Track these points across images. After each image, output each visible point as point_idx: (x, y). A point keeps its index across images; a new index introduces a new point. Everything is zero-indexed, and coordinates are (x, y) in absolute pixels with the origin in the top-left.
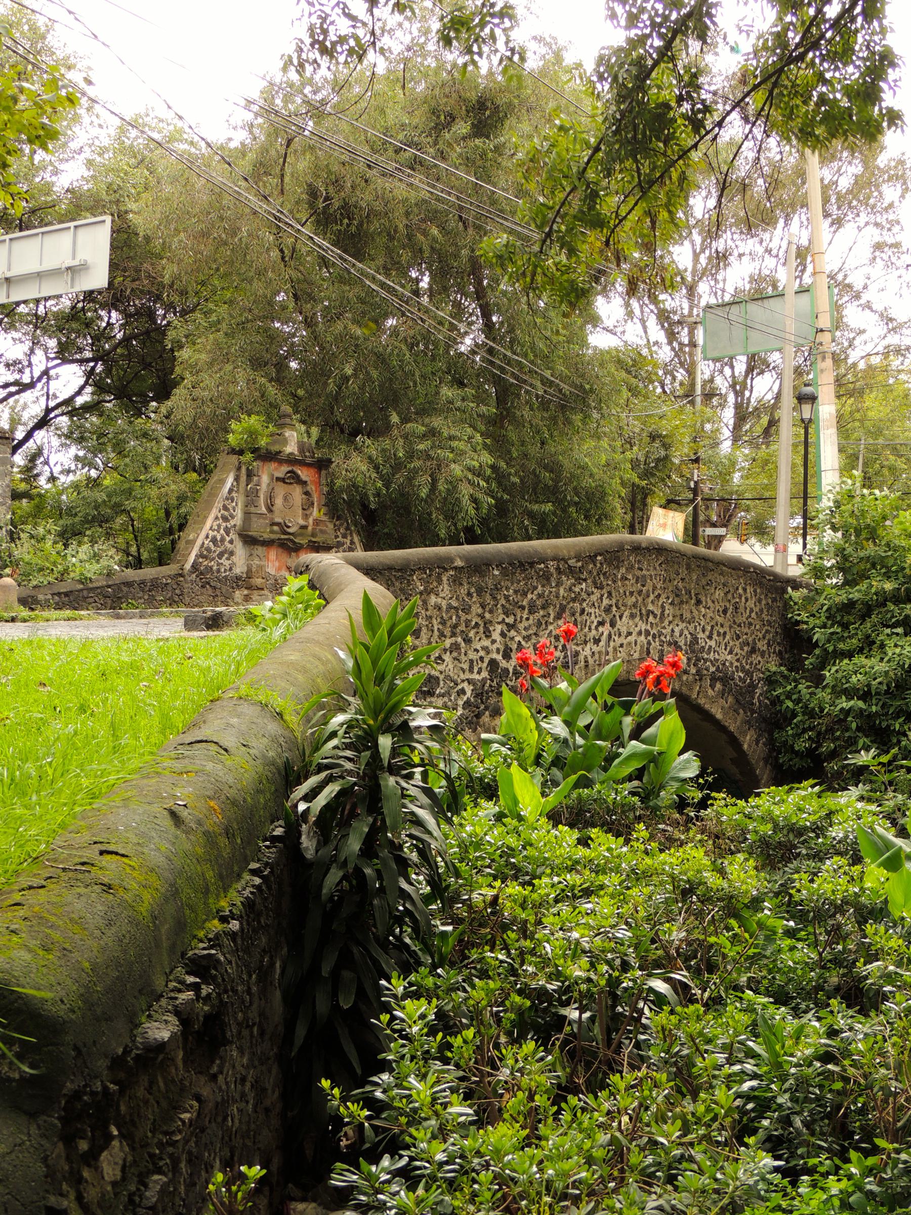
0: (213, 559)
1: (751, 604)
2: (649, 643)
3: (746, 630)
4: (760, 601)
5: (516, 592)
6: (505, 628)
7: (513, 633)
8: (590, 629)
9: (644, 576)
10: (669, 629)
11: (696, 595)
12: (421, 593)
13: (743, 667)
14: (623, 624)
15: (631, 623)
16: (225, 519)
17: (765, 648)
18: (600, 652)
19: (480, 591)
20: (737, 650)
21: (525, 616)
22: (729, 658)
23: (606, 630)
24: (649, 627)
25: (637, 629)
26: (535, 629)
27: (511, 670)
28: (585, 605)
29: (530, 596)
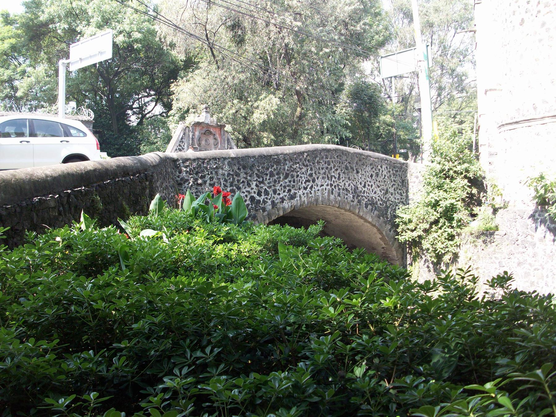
1: (385, 173)
2: (333, 189)
3: (382, 184)
4: (389, 172)
5: (262, 168)
6: (258, 183)
7: (262, 185)
8: (302, 183)
9: (329, 161)
10: (342, 184)
11: (356, 169)
12: (214, 169)
13: (381, 199)
14: (319, 182)
15: (323, 181)
17: (393, 191)
18: (307, 193)
19: (244, 168)
20: (378, 192)
21: (268, 178)
22: (374, 195)
23: (311, 184)
24: (332, 183)
25: (326, 183)
26: (273, 183)
27: (262, 201)
28: (299, 173)
29: (270, 170)
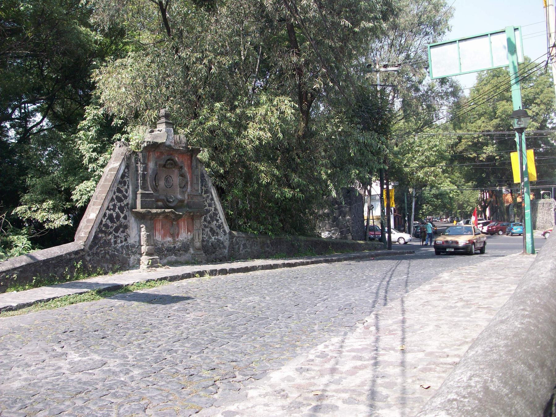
0: (111, 233)
16: (120, 200)
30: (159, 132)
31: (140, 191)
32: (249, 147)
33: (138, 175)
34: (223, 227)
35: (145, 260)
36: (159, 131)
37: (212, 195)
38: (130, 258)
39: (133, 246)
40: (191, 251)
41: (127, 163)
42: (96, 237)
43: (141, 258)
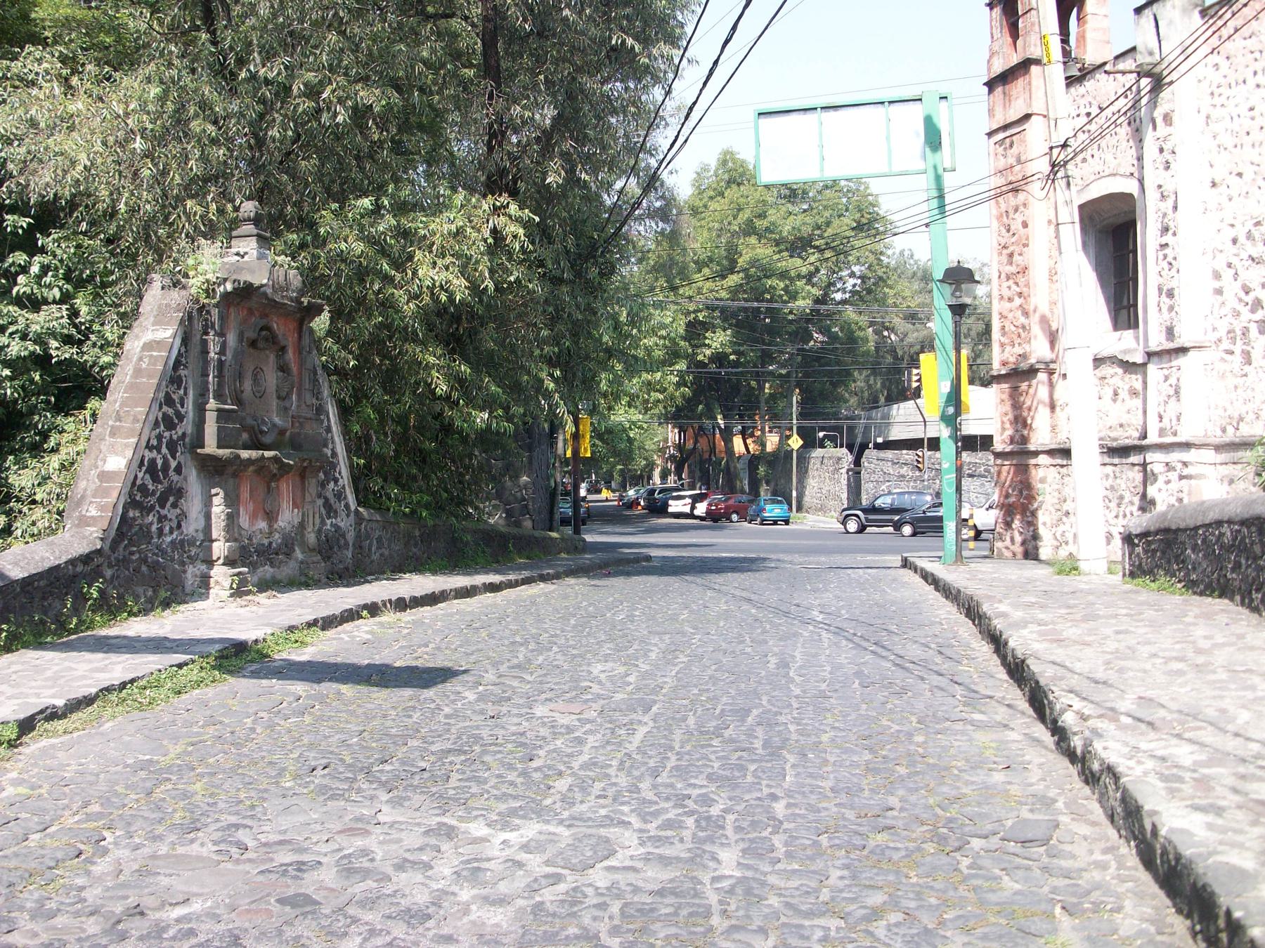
16: (170, 425)
30: (237, 258)
31: (212, 404)
32: (410, 308)
33: (206, 362)
34: (345, 498)
35: (221, 576)
36: (238, 254)
37: (329, 420)
38: (185, 572)
39: (192, 542)
40: (299, 554)
41: (185, 333)
42: (124, 517)
43: (212, 573)
